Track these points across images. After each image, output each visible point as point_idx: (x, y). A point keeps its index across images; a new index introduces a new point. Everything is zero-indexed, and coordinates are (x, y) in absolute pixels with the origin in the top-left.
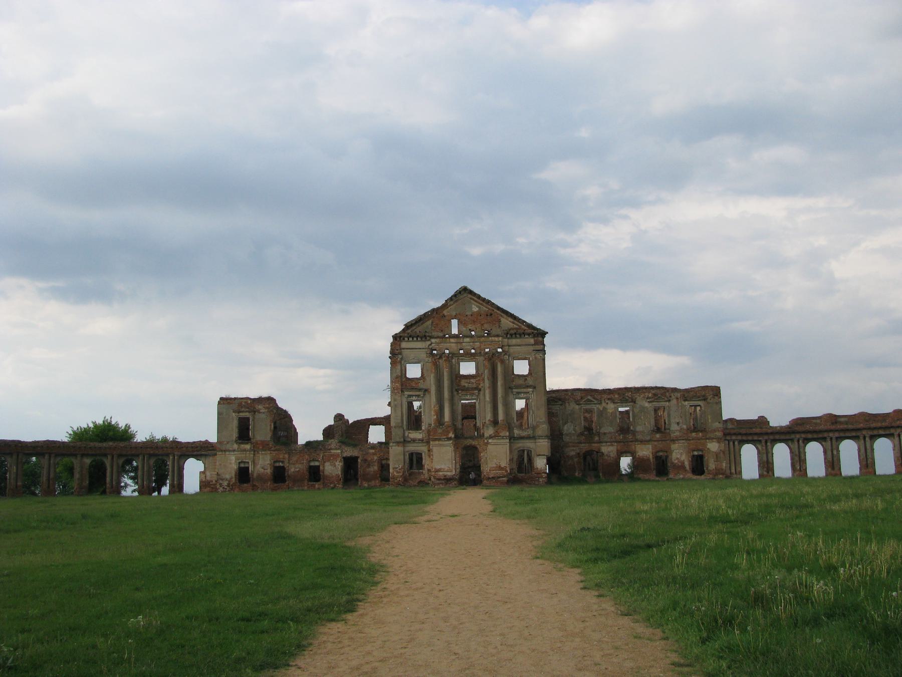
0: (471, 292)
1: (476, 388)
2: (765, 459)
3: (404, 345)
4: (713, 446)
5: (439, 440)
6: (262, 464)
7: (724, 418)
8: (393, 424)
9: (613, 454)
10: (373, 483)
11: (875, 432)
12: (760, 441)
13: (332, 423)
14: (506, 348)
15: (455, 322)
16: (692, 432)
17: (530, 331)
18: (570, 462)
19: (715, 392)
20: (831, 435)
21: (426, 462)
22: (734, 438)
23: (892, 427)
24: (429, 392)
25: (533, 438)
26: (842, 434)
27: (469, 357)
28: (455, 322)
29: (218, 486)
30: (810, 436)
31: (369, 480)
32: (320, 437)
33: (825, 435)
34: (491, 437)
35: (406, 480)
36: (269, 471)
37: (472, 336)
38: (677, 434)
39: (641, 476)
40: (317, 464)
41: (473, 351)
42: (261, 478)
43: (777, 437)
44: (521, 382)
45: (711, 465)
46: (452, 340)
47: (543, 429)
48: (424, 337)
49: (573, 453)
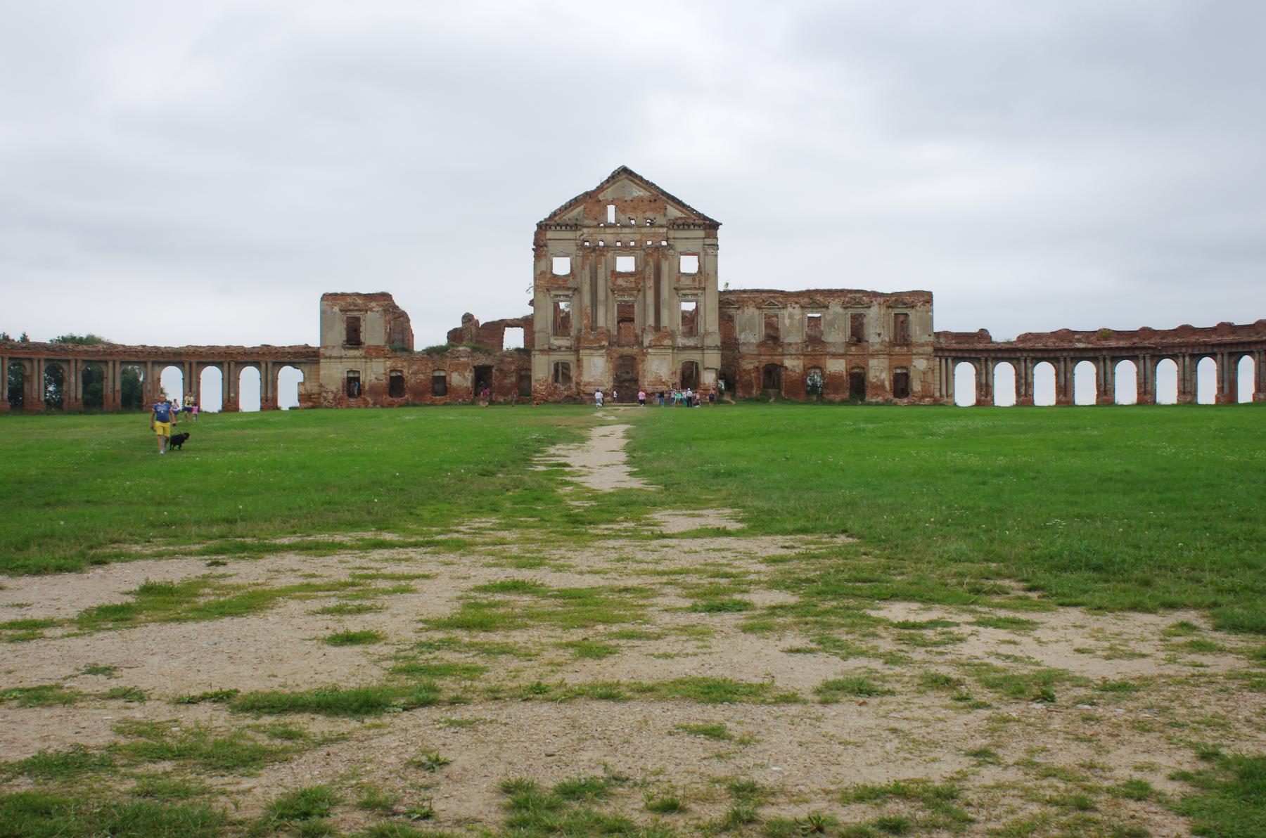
0: (631, 173)
2: (984, 381)
3: (550, 235)
4: (920, 364)
5: (590, 348)
6: (374, 372)
7: (936, 330)
8: (537, 327)
9: (799, 370)
11: (1117, 354)
12: (979, 359)
13: (459, 325)
14: (672, 242)
15: (611, 209)
16: (895, 345)
17: (701, 222)
18: (747, 377)
19: (926, 298)
20: (1065, 354)
21: (573, 373)
22: (947, 354)
23: (1137, 348)
24: (580, 292)
25: (702, 349)
26: (1077, 354)
28: (611, 209)
29: (322, 400)
30: (1039, 355)
31: (505, 394)
32: (443, 341)
33: (1058, 354)
34: (650, 347)
36: (385, 381)
37: (631, 226)
38: (877, 347)
39: (831, 396)
40: (442, 374)
41: (632, 244)
42: (374, 391)
43: (999, 355)
44: (688, 282)
45: (916, 386)
46: (608, 230)
47: (715, 340)
48: (575, 226)
49: (751, 367)
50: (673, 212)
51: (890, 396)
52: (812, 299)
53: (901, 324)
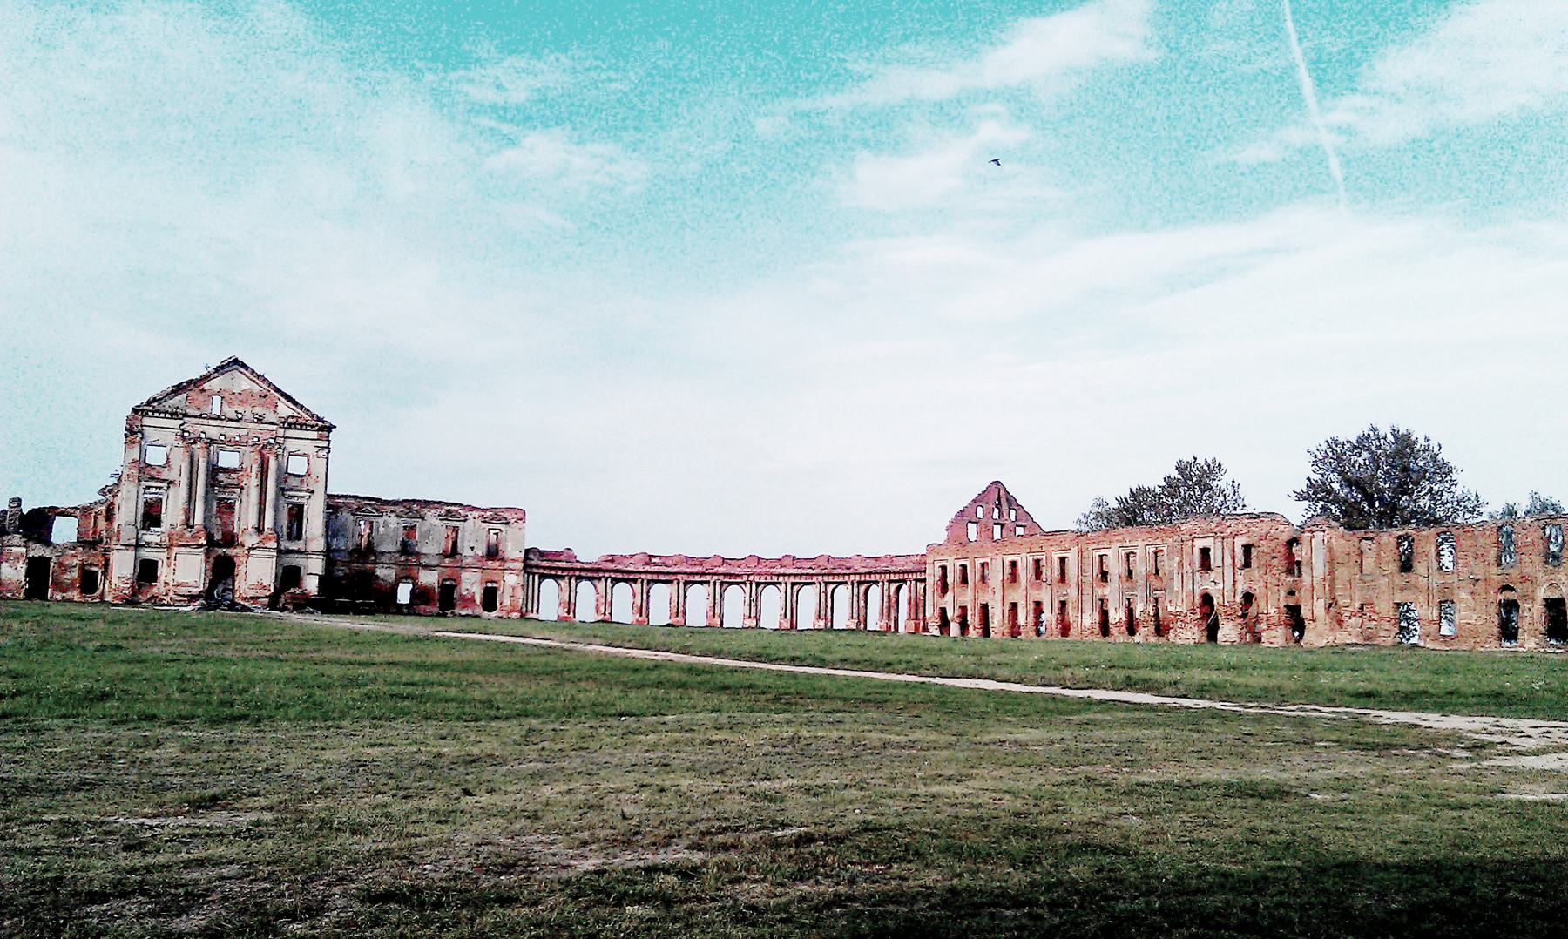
1: (237, 486)
10: (68, 595)
14: (281, 441)
15: (217, 400)
21: (162, 571)
27: (236, 444)
28: (217, 400)
35: (134, 594)
38: (469, 560)
45: (505, 600)
47: (319, 544)
50: (285, 409)
51: (479, 610)
52: (413, 508)
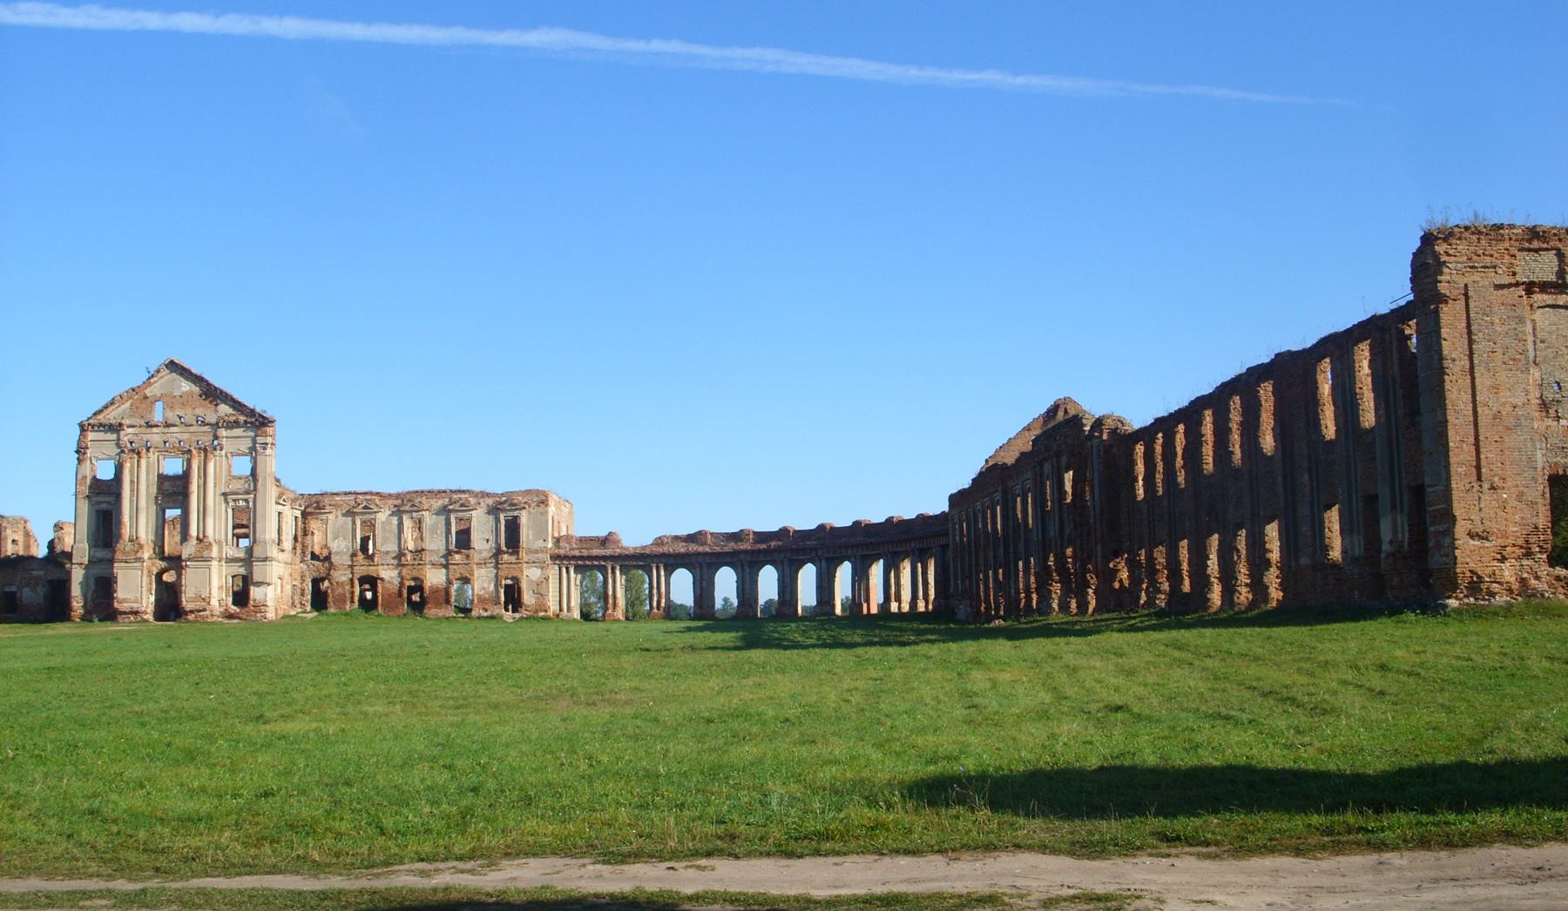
18: (340, 590)
19: (541, 500)
40: (14, 589)
45: (528, 598)
49: (344, 578)
50: (224, 409)
53: (513, 528)
